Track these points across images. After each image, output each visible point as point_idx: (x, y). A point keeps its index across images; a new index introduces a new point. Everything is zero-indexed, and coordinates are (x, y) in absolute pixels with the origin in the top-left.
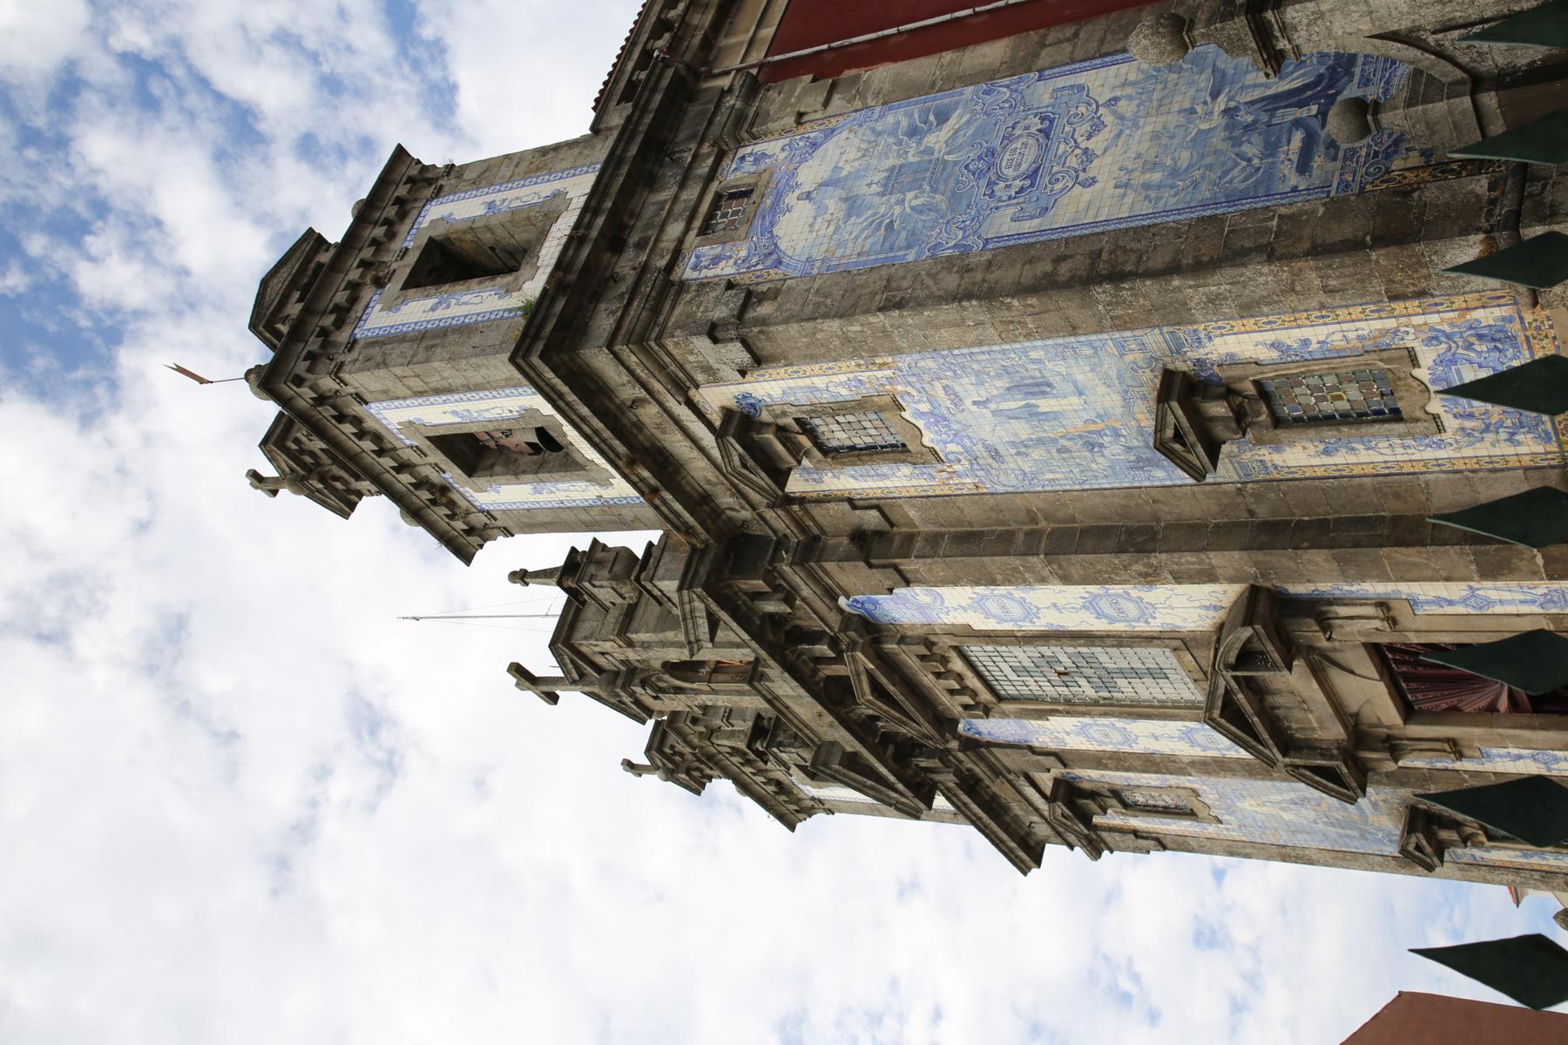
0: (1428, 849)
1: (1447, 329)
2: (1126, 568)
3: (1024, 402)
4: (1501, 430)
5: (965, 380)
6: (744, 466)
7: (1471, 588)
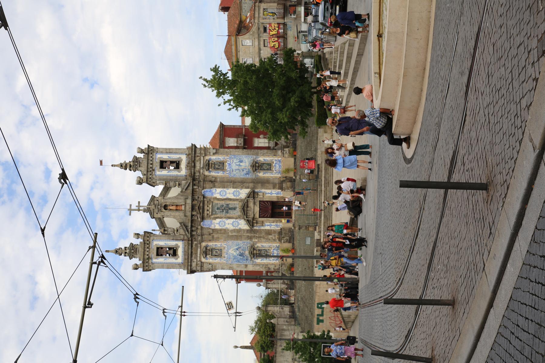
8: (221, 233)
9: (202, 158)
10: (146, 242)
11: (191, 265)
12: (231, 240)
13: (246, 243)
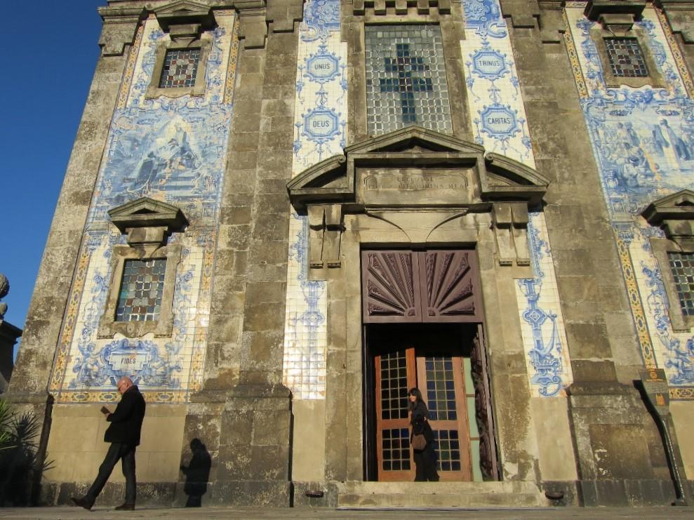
0: (145, 217)
2: (552, 139)
3: (669, 142)
4: (680, 361)
5: (684, 124)
8: (270, 63)
12: (238, 124)
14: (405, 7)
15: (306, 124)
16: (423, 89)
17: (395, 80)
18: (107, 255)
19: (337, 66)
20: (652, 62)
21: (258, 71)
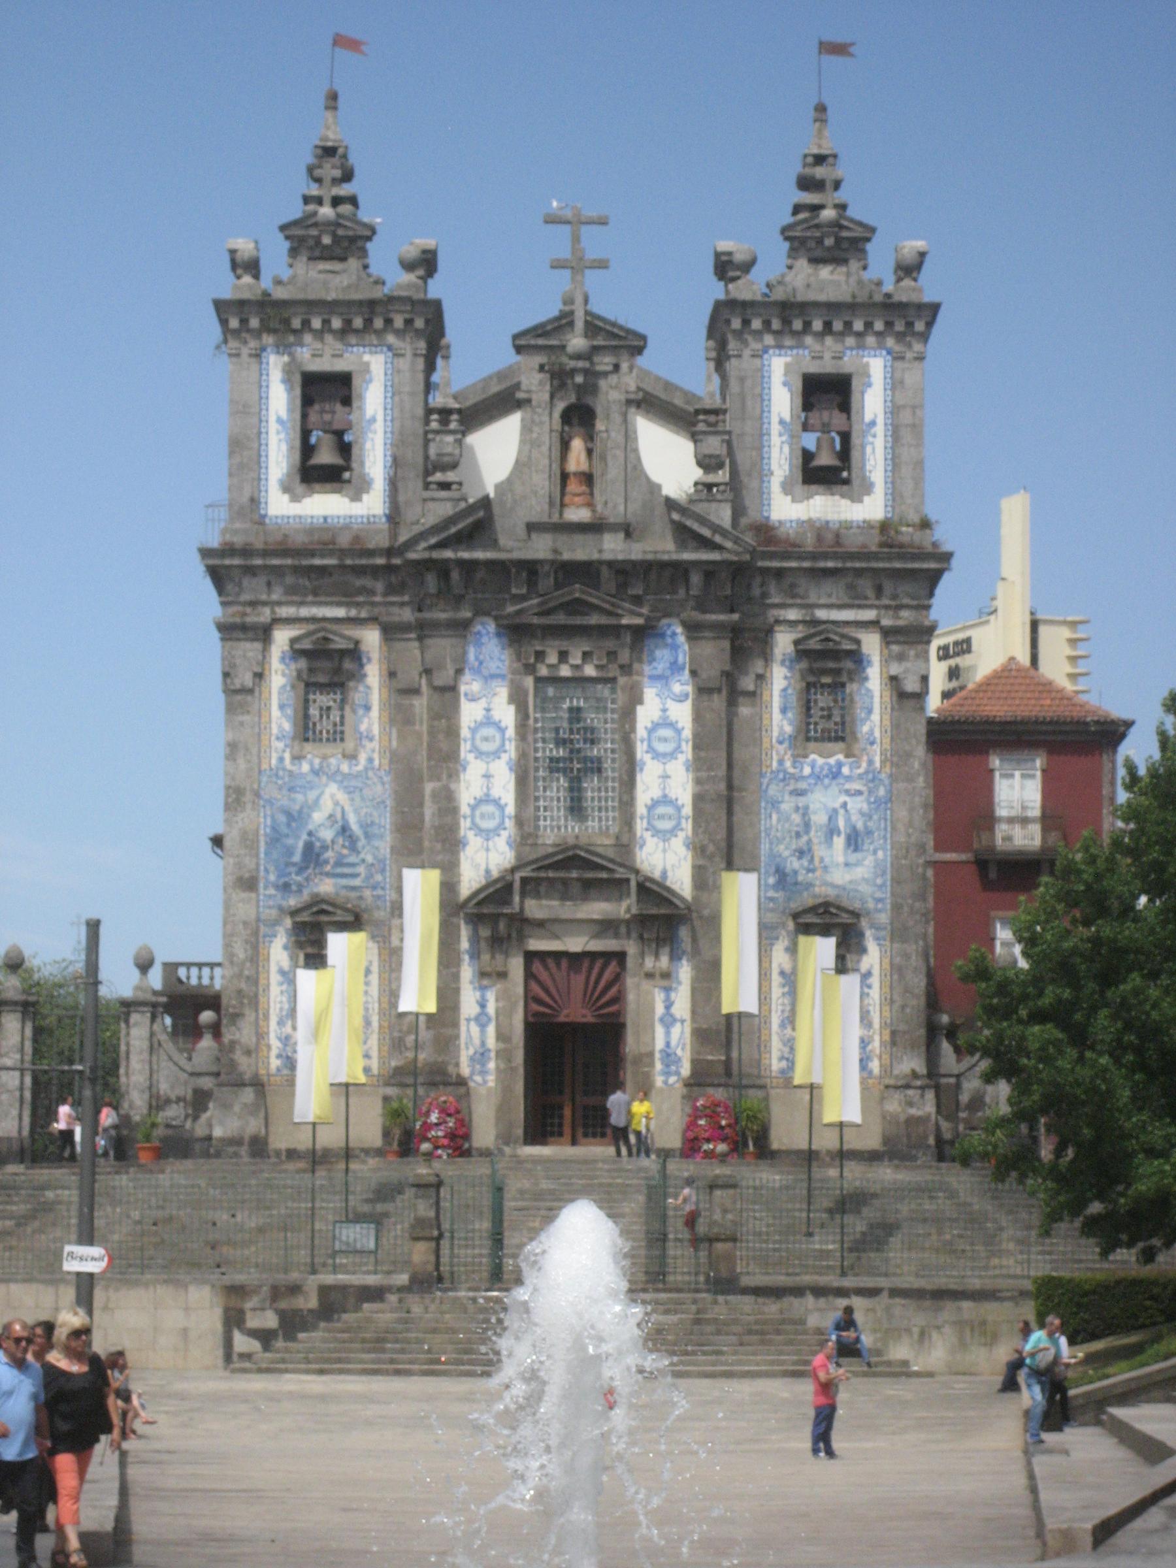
1: (870, 1047)
2: (711, 840)
5: (865, 807)
6: (828, 640)
7: (683, 1021)
8: (432, 733)
9: (869, 615)
10: (379, 309)
11: (251, 571)
13: (379, 878)
14: (579, 661)
15: (473, 817)
16: (592, 770)
17: (564, 759)
18: (285, 948)
19: (503, 740)
20: (853, 721)
21: (414, 724)
